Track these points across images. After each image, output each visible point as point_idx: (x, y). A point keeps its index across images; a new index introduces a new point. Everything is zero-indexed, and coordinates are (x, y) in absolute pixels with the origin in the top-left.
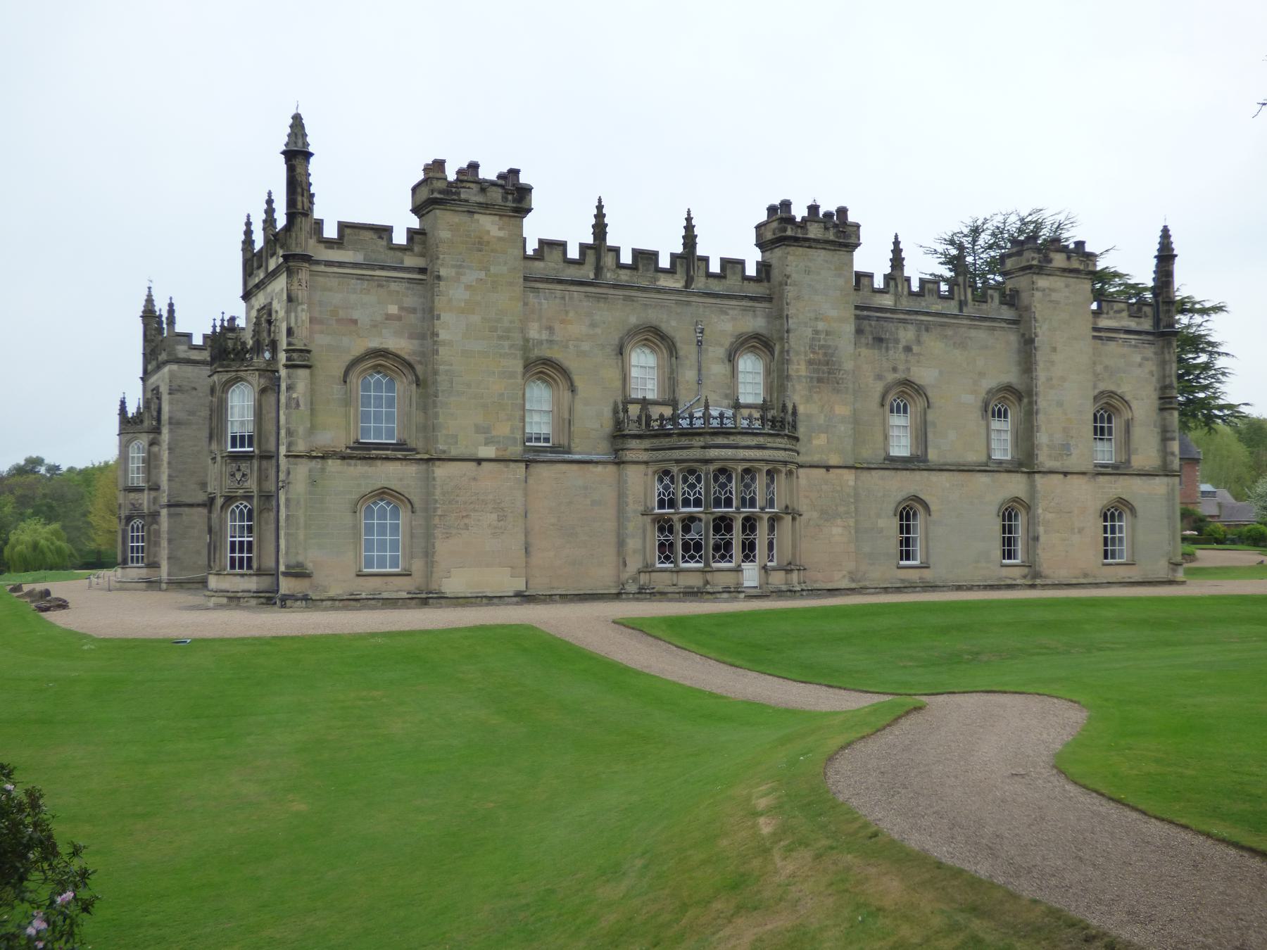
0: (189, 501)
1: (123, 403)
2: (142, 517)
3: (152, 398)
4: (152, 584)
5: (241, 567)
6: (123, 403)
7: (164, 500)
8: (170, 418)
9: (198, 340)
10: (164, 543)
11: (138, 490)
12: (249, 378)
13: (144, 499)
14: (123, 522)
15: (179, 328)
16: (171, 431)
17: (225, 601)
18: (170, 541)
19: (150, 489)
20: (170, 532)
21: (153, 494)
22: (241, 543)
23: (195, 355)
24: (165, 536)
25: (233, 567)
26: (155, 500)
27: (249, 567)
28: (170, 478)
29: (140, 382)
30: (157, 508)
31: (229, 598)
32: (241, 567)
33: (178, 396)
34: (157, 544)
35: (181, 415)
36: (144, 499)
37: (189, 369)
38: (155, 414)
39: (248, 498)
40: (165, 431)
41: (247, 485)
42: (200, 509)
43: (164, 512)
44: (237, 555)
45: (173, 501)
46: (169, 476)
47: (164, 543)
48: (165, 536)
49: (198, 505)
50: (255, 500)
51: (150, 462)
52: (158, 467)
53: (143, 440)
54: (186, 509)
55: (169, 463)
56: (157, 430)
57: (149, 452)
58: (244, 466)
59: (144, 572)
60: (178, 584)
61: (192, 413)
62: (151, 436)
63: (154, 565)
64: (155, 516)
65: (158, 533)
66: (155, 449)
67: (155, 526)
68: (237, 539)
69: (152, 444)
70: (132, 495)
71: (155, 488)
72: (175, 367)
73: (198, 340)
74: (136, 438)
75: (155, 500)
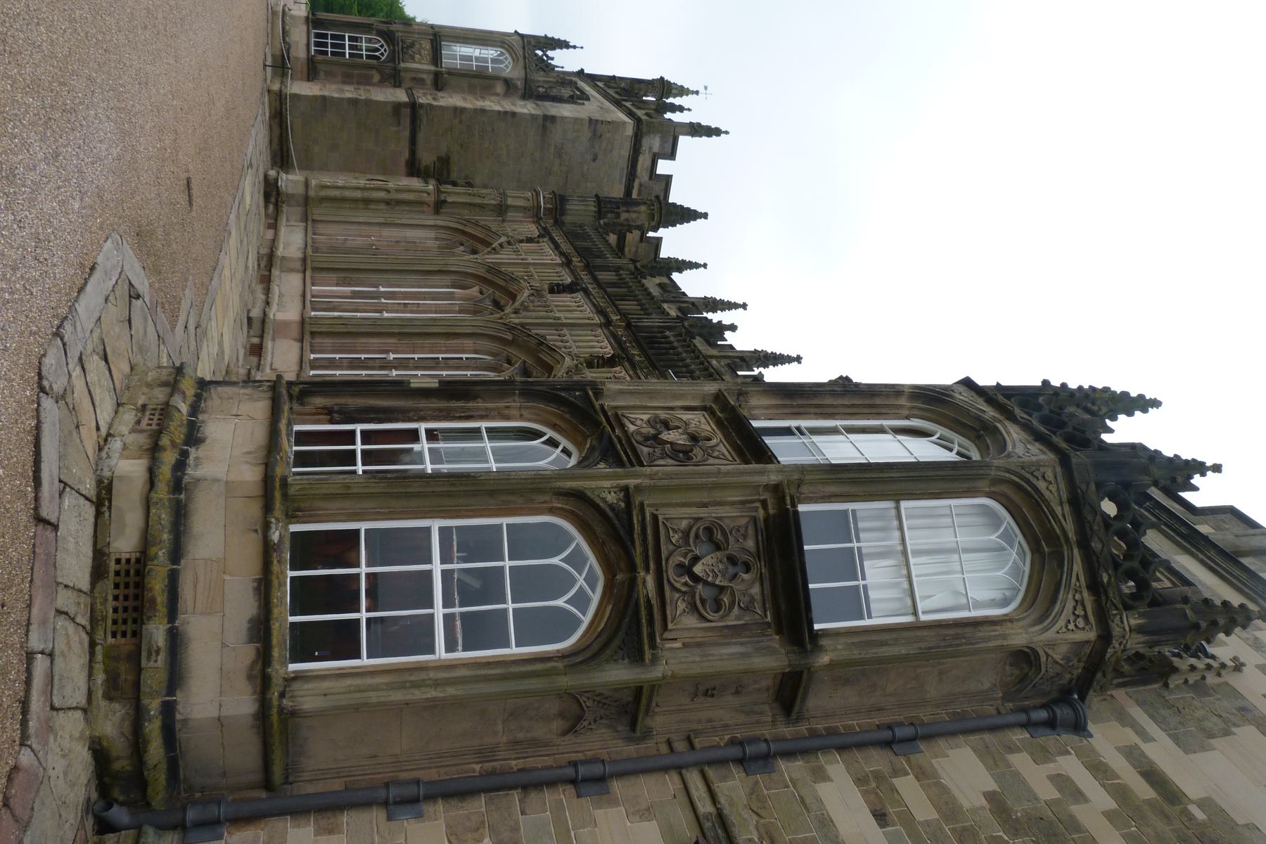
0: (421, 136)
1: (564, 45)
2: (392, 58)
3: (575, 86)
4: (281, 65)
5: (306, 595)
6: (564, 45)
7: (423, 99)
8: (553, 119)
9: (663, 167)
10: (349, 92)
11: (436, 57)
12: (1067, 601)
13: (421, 65)
14: (383, 27)
15: (684, 141)
16: (533, 117)
17: (124, 543)
18: (354, 102)
19: (437, 75)
20: (369, 103)
21: (429, 79)
22: (419, 590)
23: (644, 161)
24: (362, 94)
25: (310, 549)
26: (419, 82)
27: (309, 643)
28: (458, 111)
29: (576, 69)
30: (407, 84)
31: (143, 558)
32: (306, 595)
33: (587, 133)
34: (347, 79)
35: (556, 135)
36: (421, 65)
37: (625, 151)
38: (554, 92)
39: (628, 626)
40: (525, 108)
41: (685, 623)
42: (406, 155)
43: (401, 96)
44: (359, 447)
45: (422, 112)
46: (463, 110)
47: (349, 92)
48: (362, 94)
49: (413, 153)
50: (618, 674)
51: (478, 80)
52: (472, 90)
53: (509, 68)
54: (407, 133)
55: (483, 111)
56: (529, 93)
57: (495, 78)
58: (751, 586)
59: (299, 52)
60: (279, 111)
61: (559, 155)
62: (520, 84)
63: (312, 71)
64: (394, 78)
65: (367, 81)
66: (500, 88)
67: (377, 78)
68: (437, 568)
69: (508, 83)
70: (427, 45)
71: (440, 81)
72: (629, 131)
73: (663, 167)
74: (515, 60)
75: (419, 82)
